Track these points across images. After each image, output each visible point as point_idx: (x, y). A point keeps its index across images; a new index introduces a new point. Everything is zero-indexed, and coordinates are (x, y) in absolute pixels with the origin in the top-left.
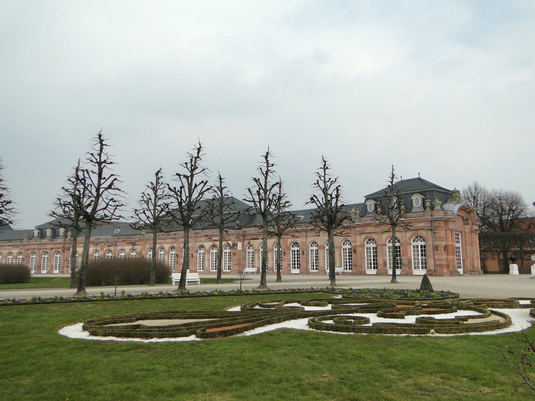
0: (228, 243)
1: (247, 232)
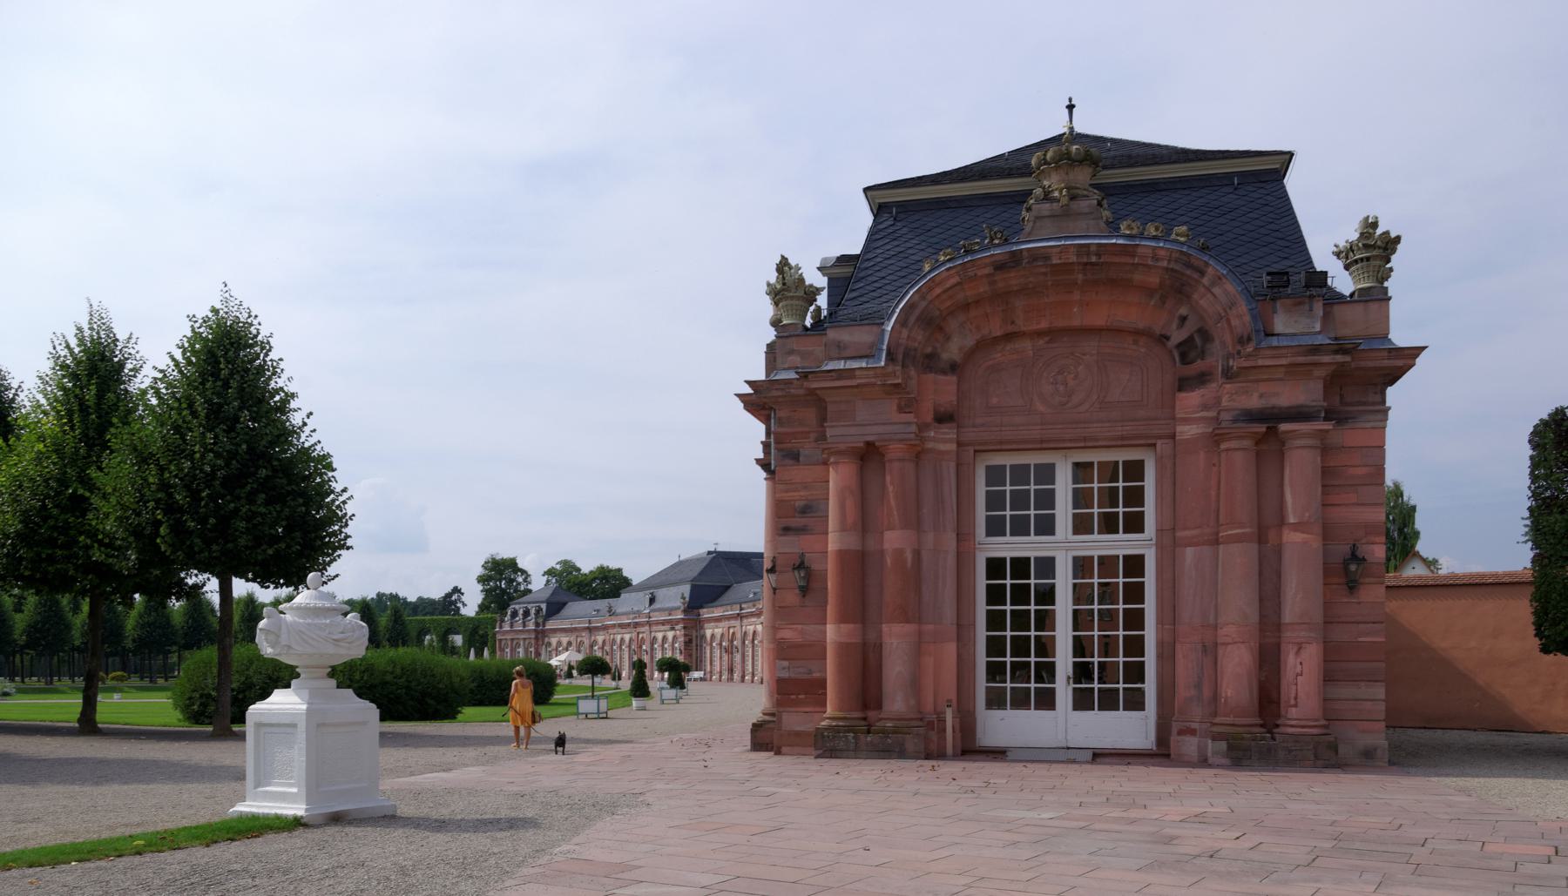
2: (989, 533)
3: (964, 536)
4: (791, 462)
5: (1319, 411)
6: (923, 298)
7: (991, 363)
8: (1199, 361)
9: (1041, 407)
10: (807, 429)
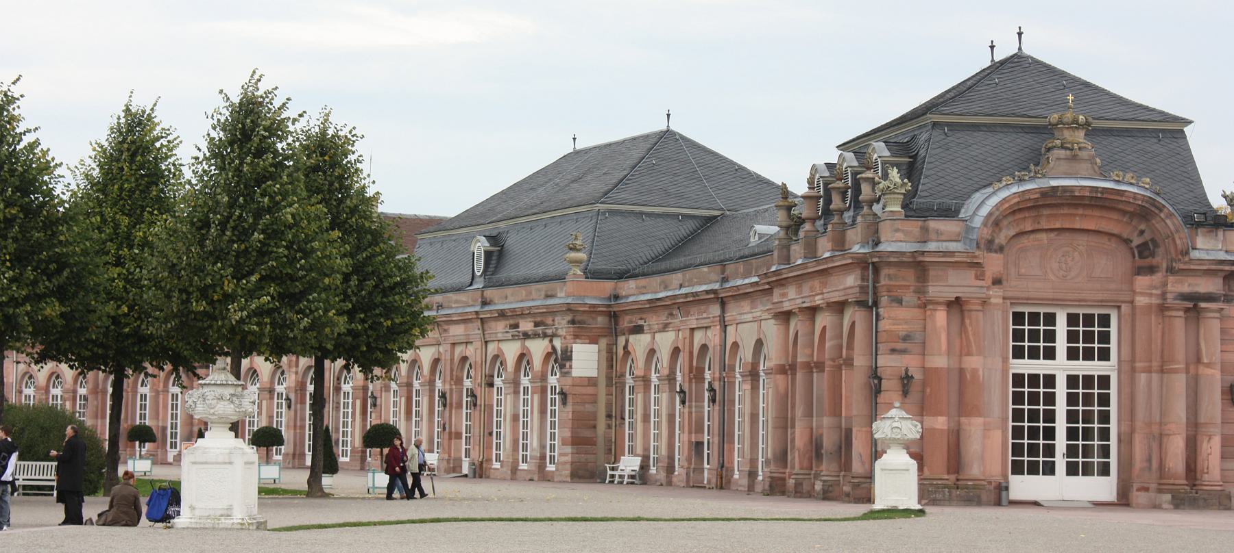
0: (554, 348)
1: (627, 297)
2: (1014, 357)
3: (1005, 360)
4: (896, 305)
6: (997, 210)
7: (1021, 245)
8: (1150, 258)
9: (1051, 277)
10: (908, 284)
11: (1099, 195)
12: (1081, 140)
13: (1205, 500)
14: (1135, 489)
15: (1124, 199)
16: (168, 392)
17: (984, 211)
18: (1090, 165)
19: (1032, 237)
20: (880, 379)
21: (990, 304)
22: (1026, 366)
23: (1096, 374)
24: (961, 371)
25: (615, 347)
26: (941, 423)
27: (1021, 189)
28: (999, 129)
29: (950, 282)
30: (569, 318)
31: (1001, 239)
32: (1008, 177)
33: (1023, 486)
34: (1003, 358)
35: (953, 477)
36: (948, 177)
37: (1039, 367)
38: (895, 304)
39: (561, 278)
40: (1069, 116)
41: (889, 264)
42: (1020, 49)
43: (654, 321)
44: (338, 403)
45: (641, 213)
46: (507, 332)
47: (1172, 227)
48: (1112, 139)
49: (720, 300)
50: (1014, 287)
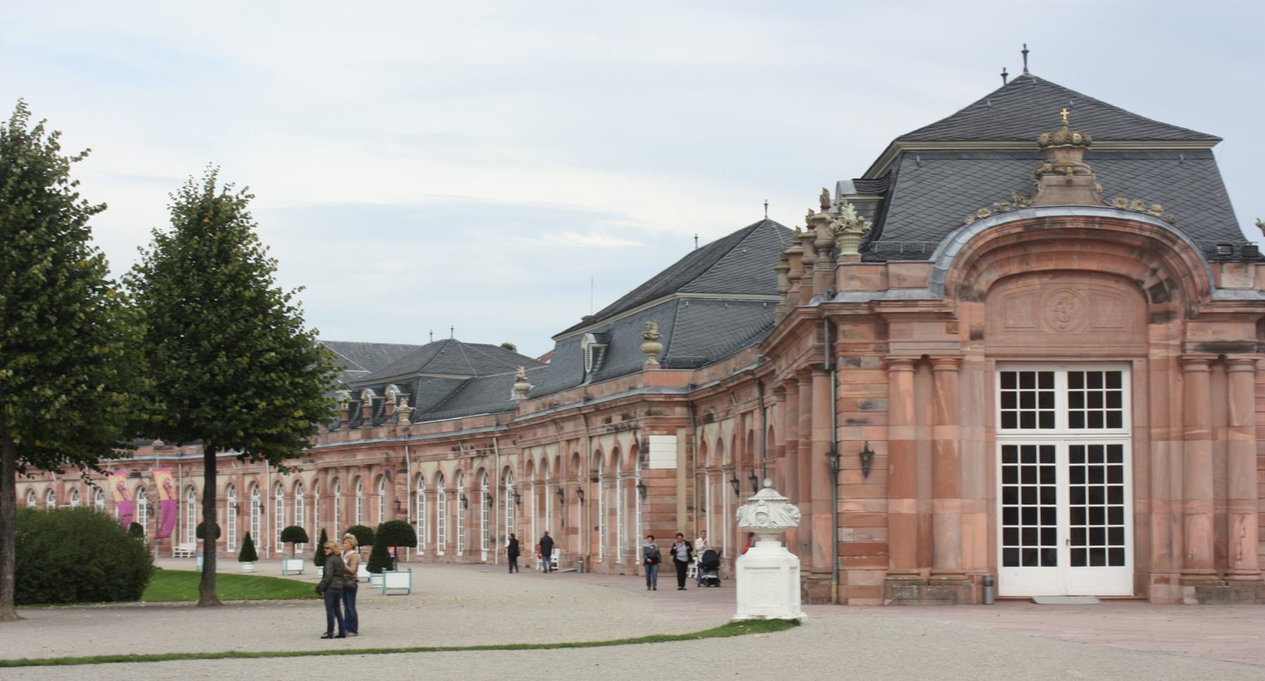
0: (637, 440)
3: (990, 430)
5: (1253, 346)
6: (970, 248)
7: (1008, 292)
8: (1166, 302)
9: (1046, 329)
10: (866, 341)
11: (1097, 227)
12: (1077, 163)
13: (1238, 592)
14: (1152, 581)
15: (1127, 230)
16: (355, 496)
17: (954, 251)
18: (1088, 192)
19: (1021, 283)
20: (838, 456)
21: (969, 362)
22: (1020, 437)
23: (1105, 443)
24: (934, 444)
25: (694, 437)
26: (906, 506)
27: (1000, 222)
28: (983, 156)
29: (916, 337)
30: (645, 409)
31: (982, 284)
32: (985, 209)
33: (1015, 580)
34: (987, 427)
35: (925, 572)
36: (920, 215)
37: (1036, 437)
38: (851, 366)
39: (638, 370)
40: (1061, 135)
41: (844, 318)
42: (1025, 70)
43: (719, 409)
44: (504, 502)
45: (724, 301)
46: (603, 427)
47: (1189, 262)
48: (1122, 163)
49: (757, 381)
50: (998, 341)
